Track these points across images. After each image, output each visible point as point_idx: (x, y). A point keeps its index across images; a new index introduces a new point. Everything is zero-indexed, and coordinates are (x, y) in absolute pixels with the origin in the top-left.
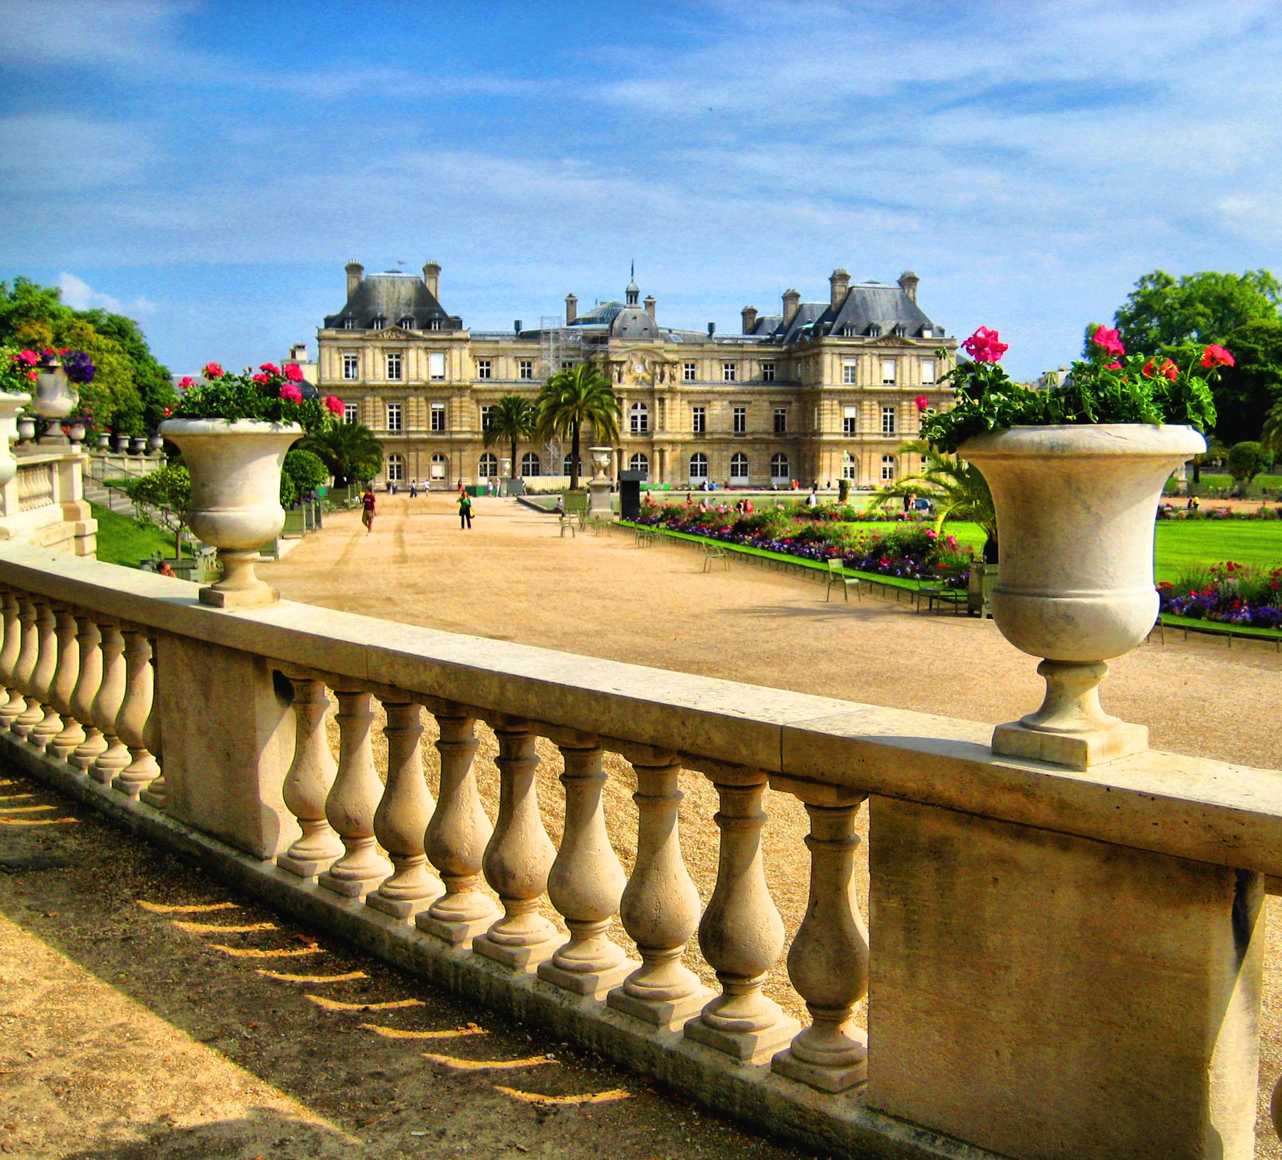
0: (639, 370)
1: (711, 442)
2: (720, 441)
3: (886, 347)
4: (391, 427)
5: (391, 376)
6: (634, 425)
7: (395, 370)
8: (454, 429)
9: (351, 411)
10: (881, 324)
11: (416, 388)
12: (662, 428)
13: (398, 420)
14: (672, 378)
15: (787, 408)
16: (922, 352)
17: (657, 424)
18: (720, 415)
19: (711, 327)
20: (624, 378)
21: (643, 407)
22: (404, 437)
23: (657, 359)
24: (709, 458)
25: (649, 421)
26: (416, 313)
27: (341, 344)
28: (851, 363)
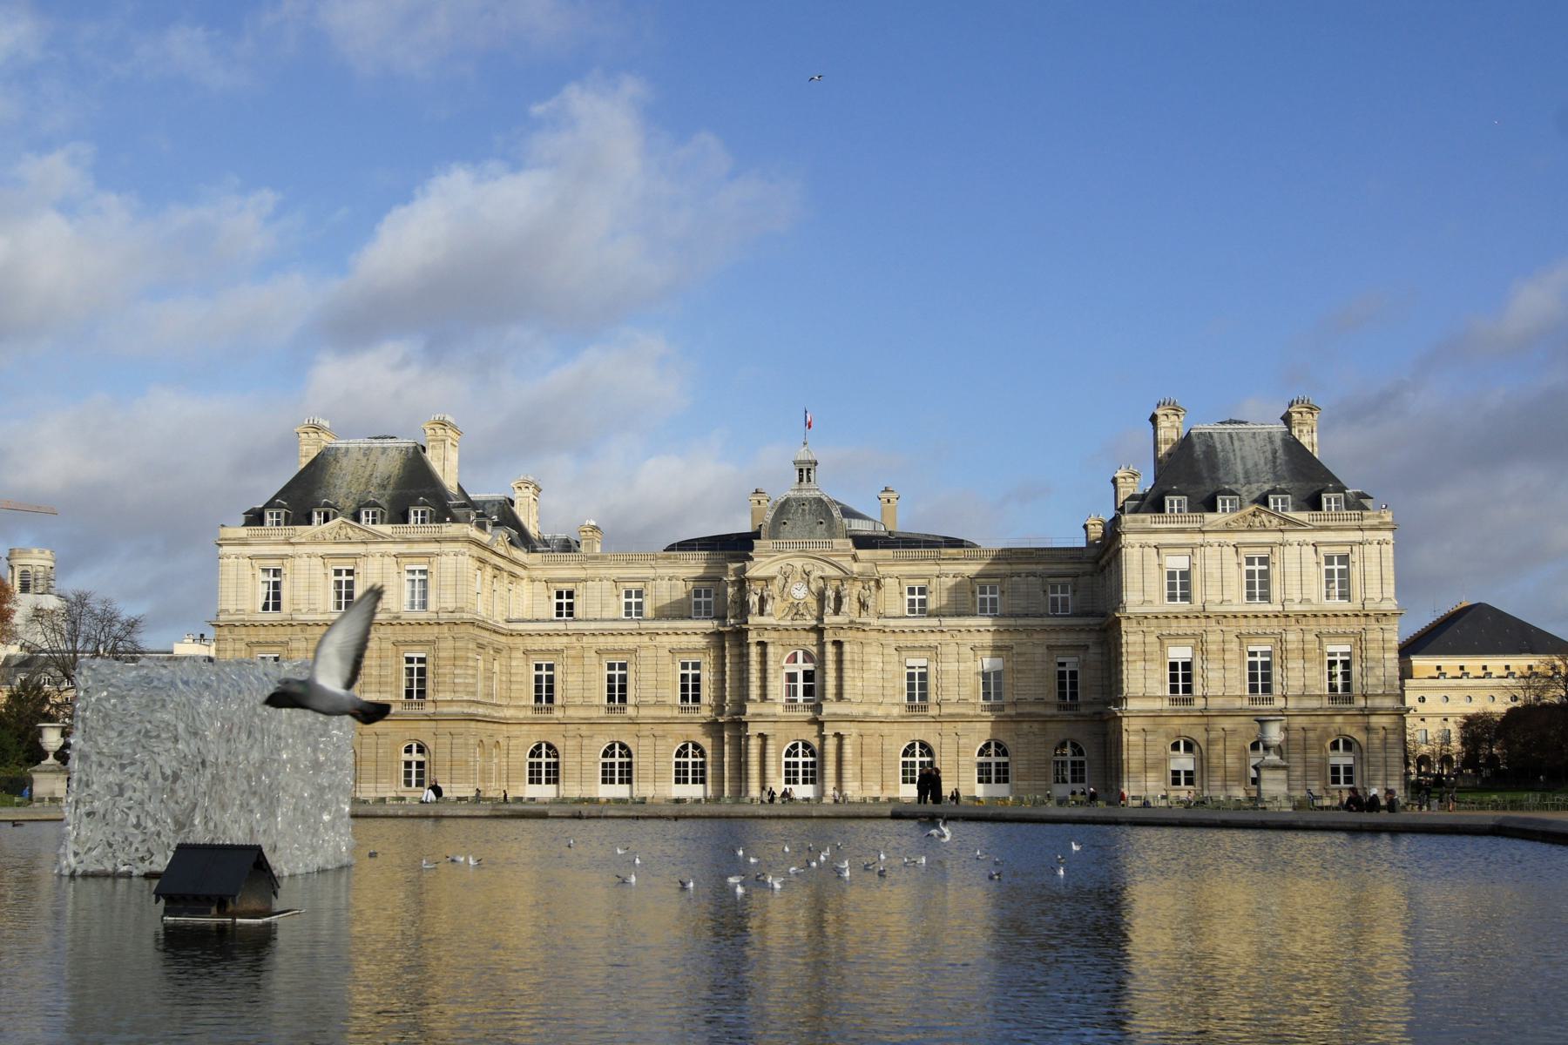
0: (799, 592)
1: (937, 720)
2: (954, 718)
3: (1250, 529)
6: (792, 691)
8: (440, 697)
10: (1244, 491)
12: (840, 696)
14: (863, 605)
17: (831, 690)
20: (768, 608)
21: (808, 657)
23: (830, 571)
24: (936, 750)
25: (816, 683)
28: (1179, 562)
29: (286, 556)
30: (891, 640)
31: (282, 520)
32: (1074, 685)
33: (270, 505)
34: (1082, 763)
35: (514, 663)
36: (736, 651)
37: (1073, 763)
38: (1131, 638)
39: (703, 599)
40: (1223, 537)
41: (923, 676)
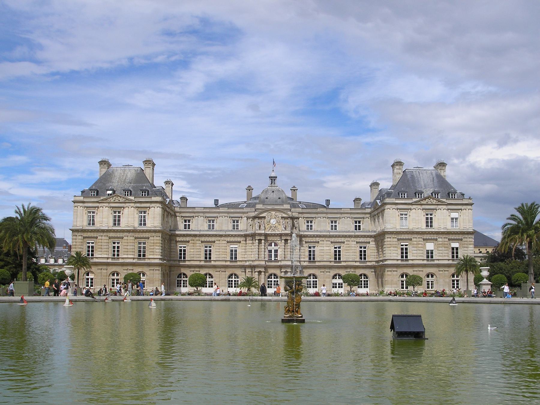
4: (114, 255)
5: (115, 224)
7: (117, 221)
9: (91, 245)
10: (424, 191)
11: (129, 231)
13: (118, 251)
15: (368, 245)
16: (450, 207)
18: (324, 251)
19: (328, 201)
21: (276, 245)
22: (121, 261)
23: (284, 215)
24: (318, 277)
25: (279, 253)
26: (133, 187)
27: (86, 205)
29: (98, 207)
30: (303, 239)
31: (95, 194)
32: (365, 255)
33: (91, 190)
34: (367, 281)
35: (172, 245)
36: (251, 242)
37: (364, 281)
38: (389, 240)
39: (236, 224)
40: (419, 207)
41: (314, 251)
